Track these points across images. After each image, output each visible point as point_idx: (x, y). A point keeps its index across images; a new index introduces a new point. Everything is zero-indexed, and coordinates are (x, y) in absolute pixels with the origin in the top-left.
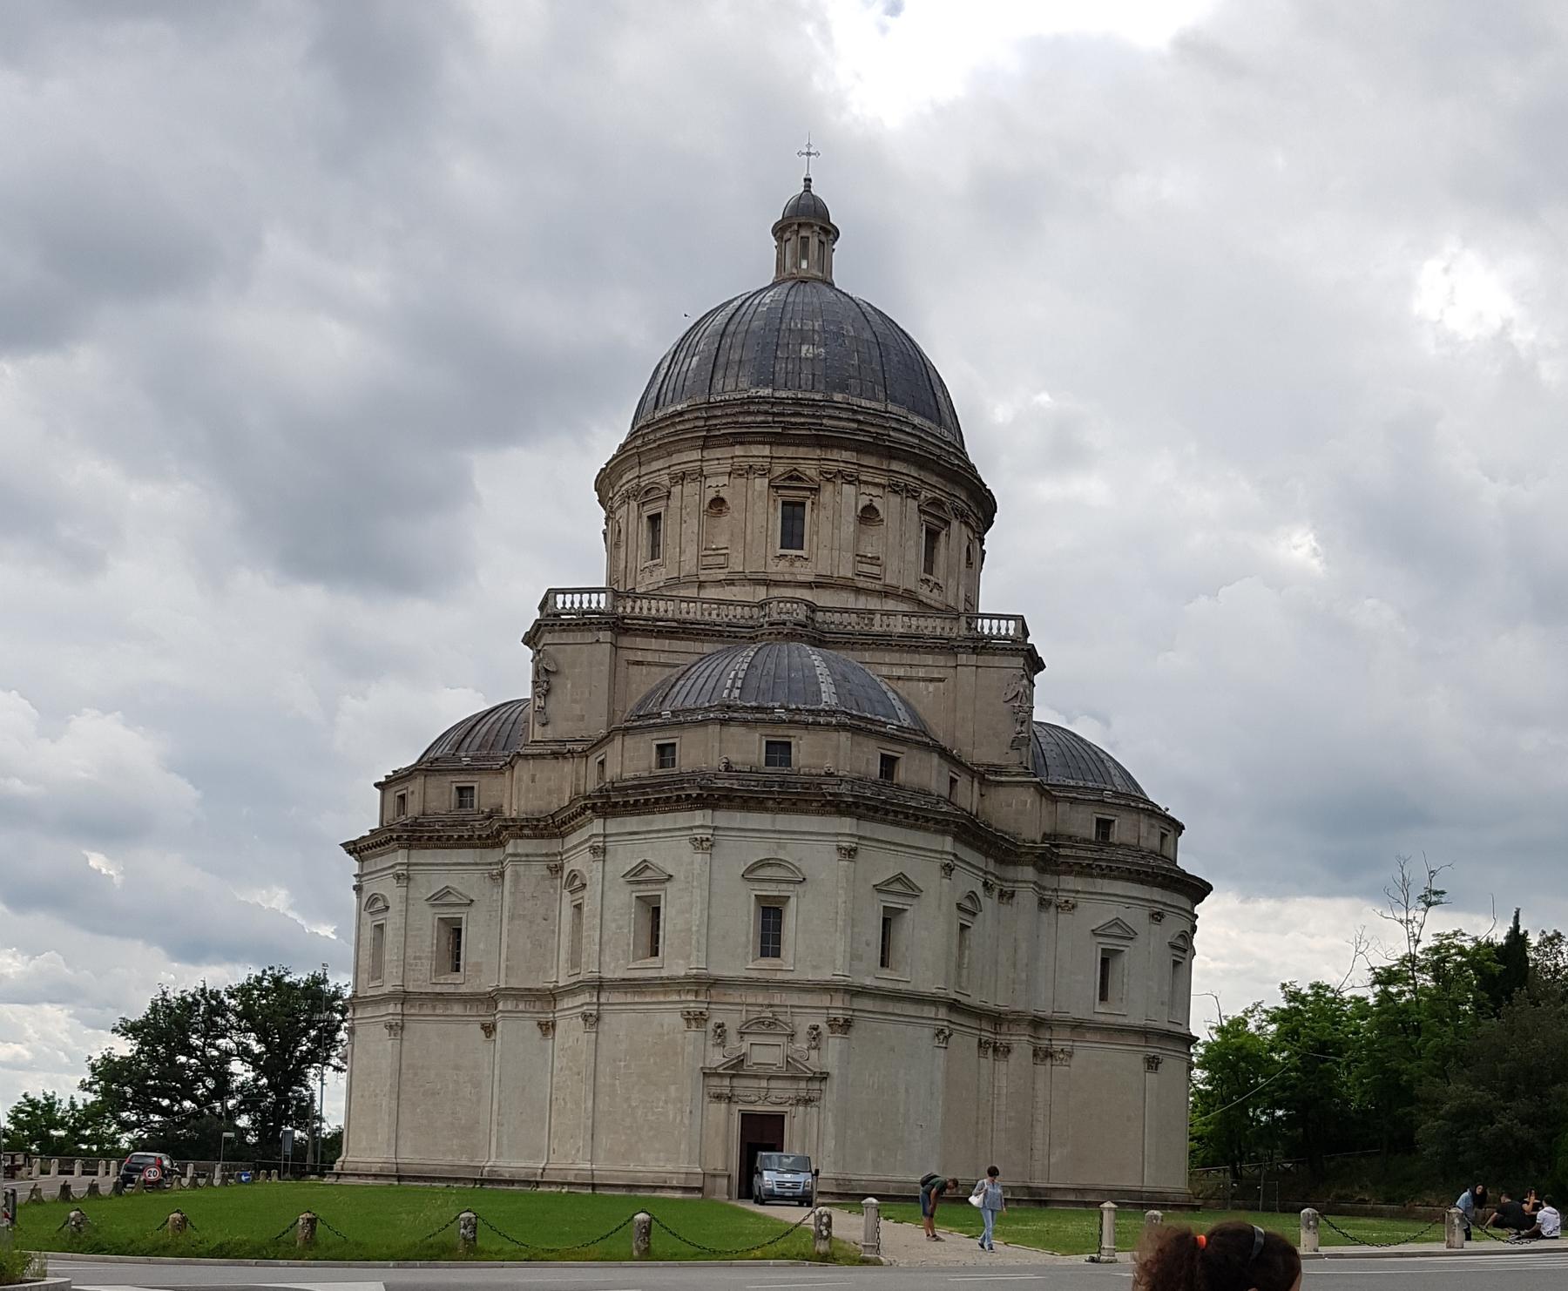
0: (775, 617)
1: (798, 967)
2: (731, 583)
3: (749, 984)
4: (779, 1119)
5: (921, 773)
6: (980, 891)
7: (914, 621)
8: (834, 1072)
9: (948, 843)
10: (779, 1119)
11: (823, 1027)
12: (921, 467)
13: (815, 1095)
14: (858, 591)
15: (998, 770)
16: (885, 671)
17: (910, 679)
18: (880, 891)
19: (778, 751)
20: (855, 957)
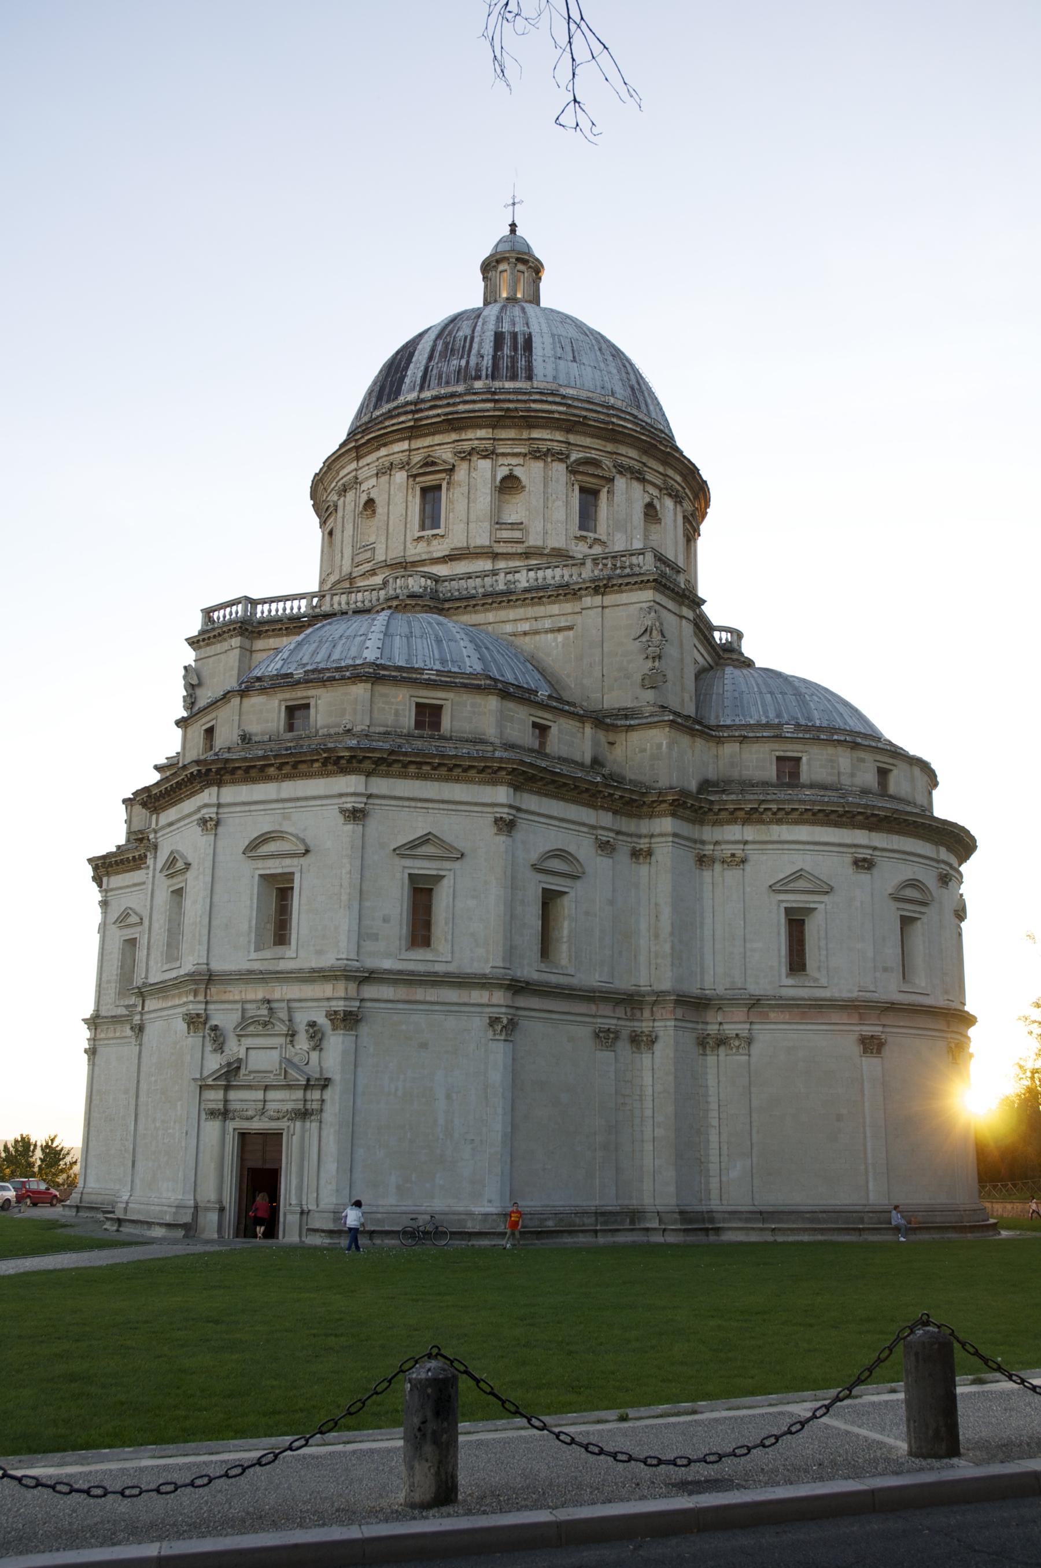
0: (391, 592)
1: (301, 952)
2: (373, 572)
4: (273, 1140)
5: (475, 717)
6: (583, 848)
7: (540, 574)
8: (337, 1077)
9: (502, 794)
10: (273, 1140)
11: (322, 1020)
12: (568, 431)
13: (316, 1106)
14: (495, 556)
15: (627, 714)
16: (509, 628)
17: (536, 632)
18: (403, 856)
20: (362, 935)
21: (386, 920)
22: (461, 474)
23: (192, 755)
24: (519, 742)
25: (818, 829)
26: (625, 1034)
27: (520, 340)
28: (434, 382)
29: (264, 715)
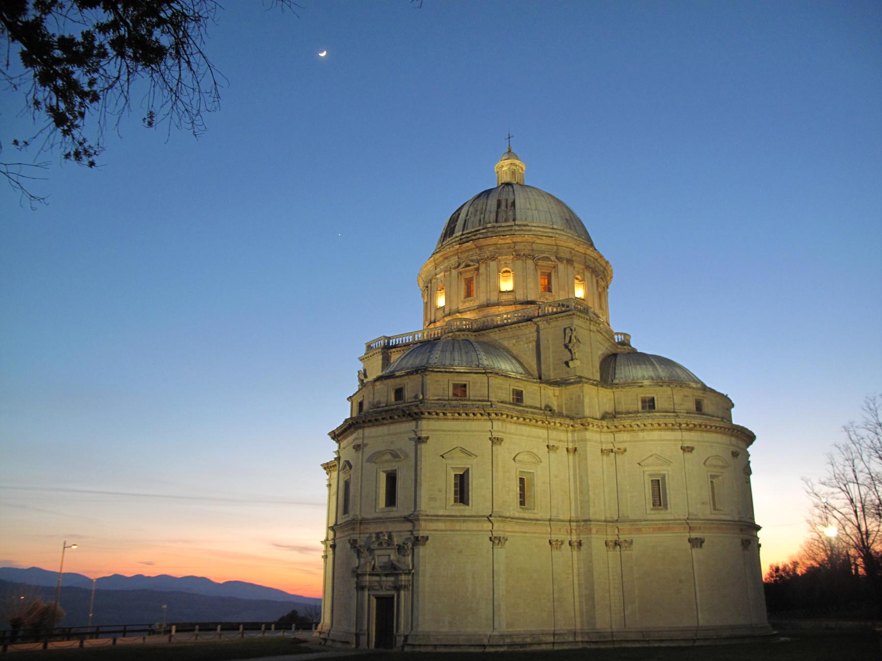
3: (377, 520)
19: (399, 393)
21: (440, 491)
22: (482, 269)
23: (355, 415)
24: (507, 399)
25: (663, 433)
26: (567, 543)
27: (510, 202)
28: (470, 225)
29: (385, 394)
